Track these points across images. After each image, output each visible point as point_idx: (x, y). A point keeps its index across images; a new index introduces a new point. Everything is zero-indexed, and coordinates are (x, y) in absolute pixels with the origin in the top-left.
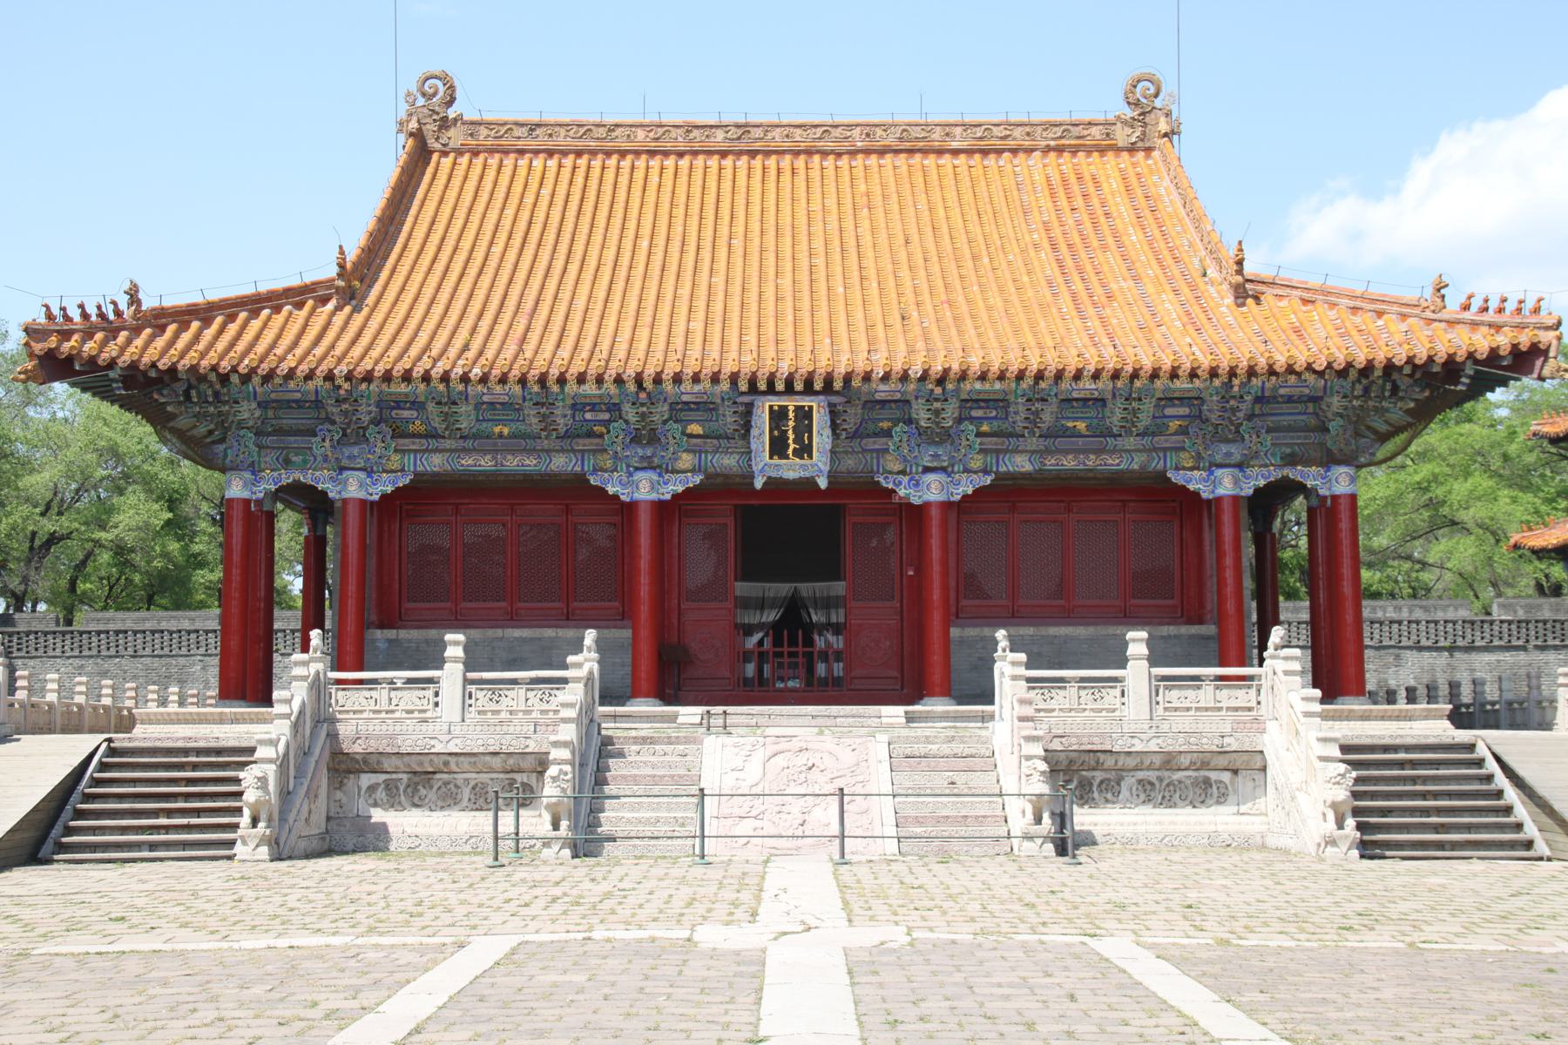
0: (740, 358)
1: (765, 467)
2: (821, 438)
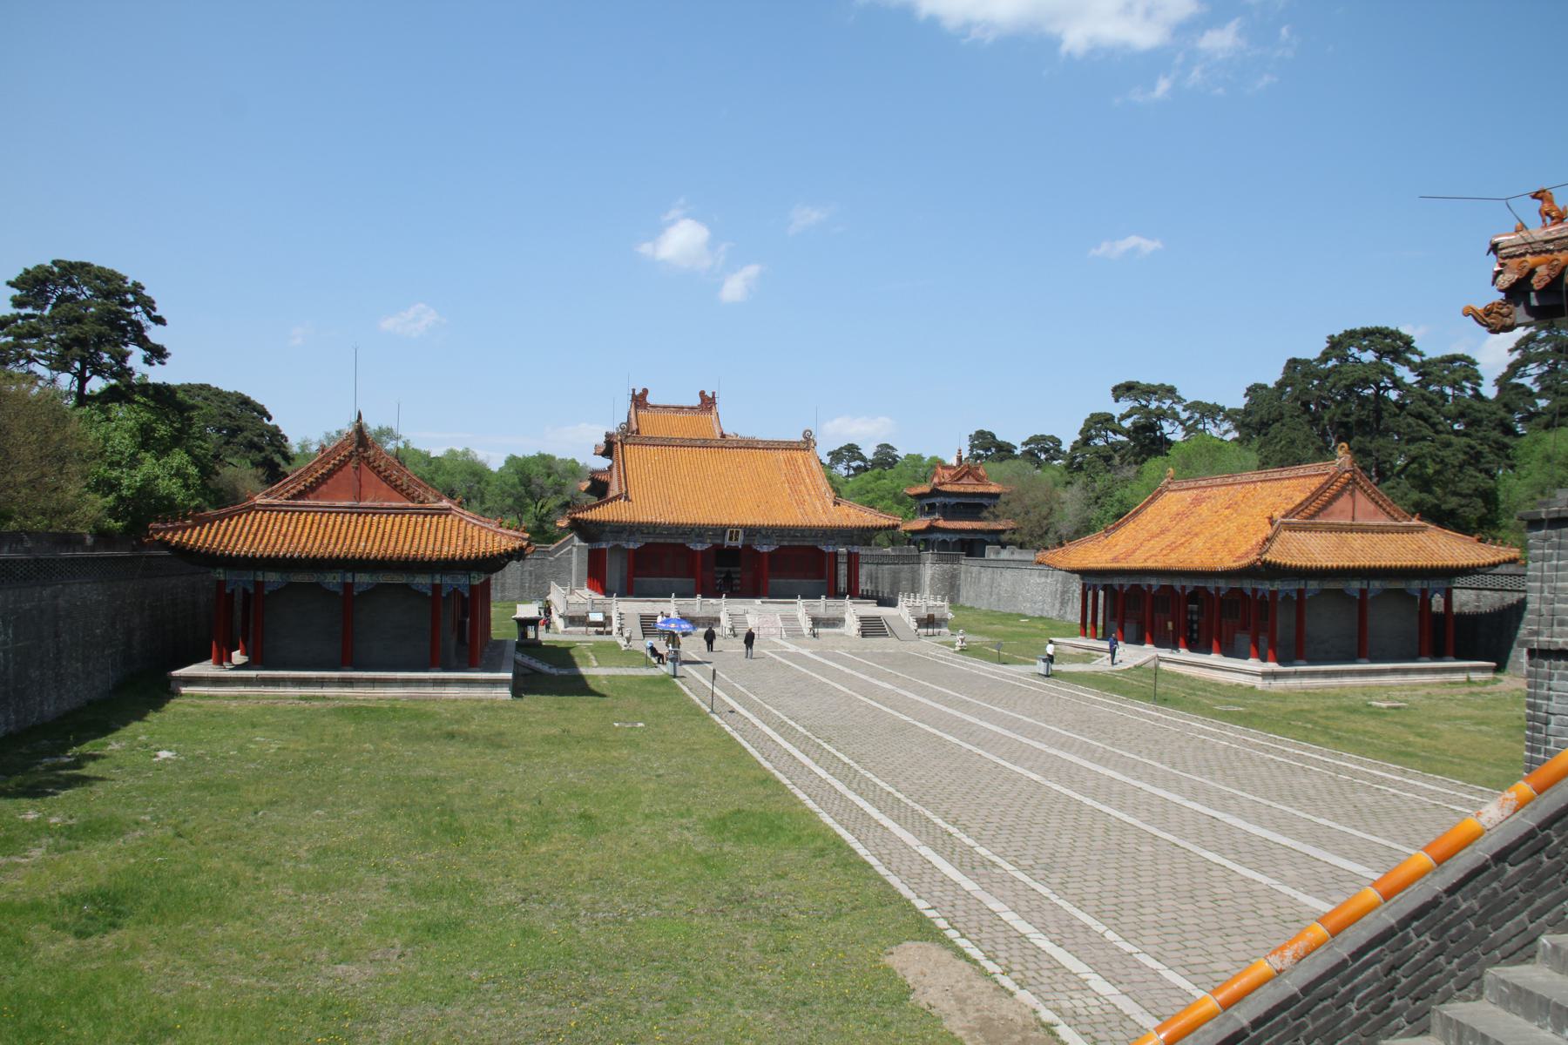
0: (726, 521)
1: (727, 542)
2: (741, 537)
